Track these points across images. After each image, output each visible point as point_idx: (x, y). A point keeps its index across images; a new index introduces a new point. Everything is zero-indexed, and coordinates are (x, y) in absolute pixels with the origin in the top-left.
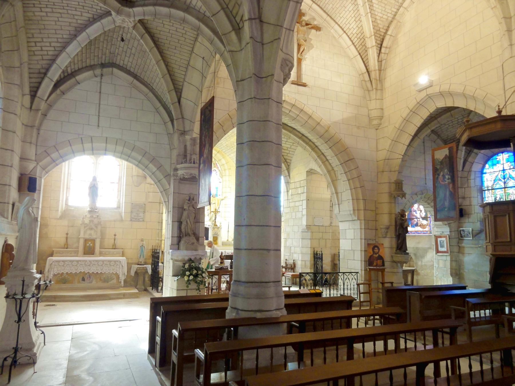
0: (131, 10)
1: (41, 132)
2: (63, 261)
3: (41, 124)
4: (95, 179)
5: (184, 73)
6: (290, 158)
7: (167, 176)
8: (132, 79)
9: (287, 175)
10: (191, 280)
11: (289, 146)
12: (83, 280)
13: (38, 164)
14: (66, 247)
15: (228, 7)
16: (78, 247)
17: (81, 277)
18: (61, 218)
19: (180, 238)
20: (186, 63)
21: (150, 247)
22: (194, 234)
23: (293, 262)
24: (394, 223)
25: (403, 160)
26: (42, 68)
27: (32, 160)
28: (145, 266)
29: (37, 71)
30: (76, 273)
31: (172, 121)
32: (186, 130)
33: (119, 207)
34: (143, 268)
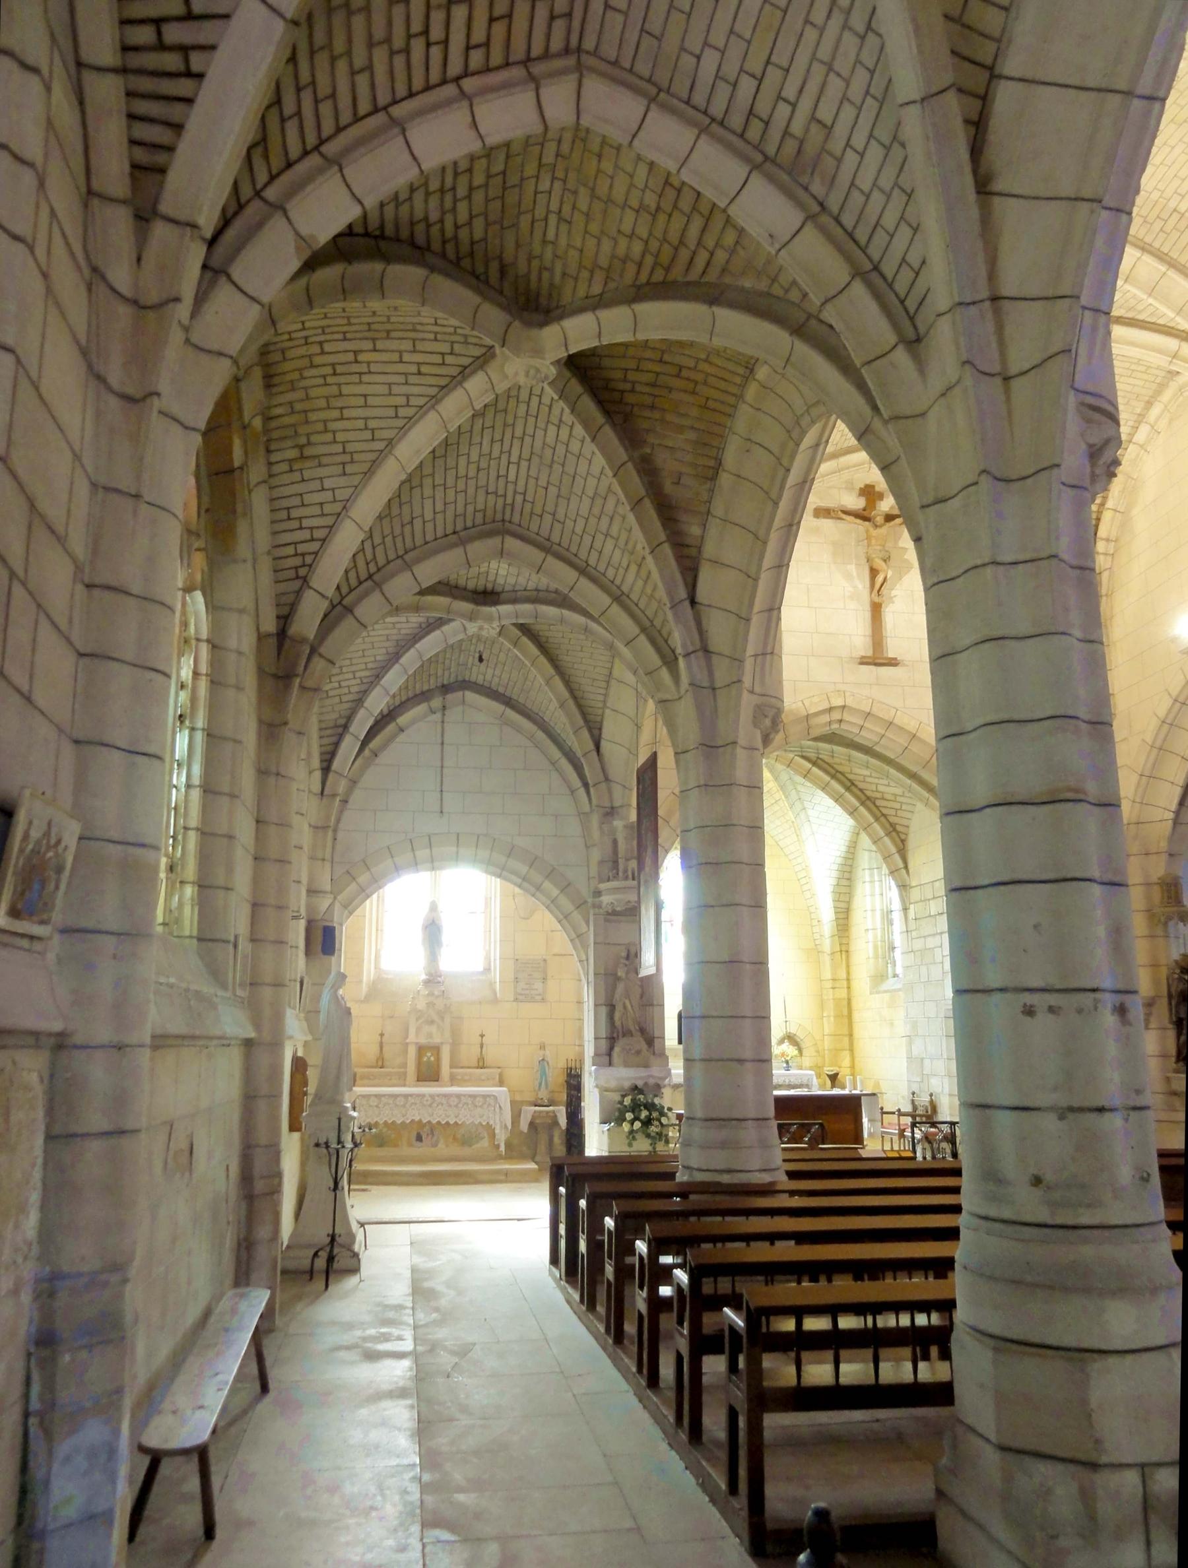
0: (493, 609)
1: (340, 835)
2: (376, 1096)
3: (338, 821)
4: (433, 908)
5: (603, 691)
6: (905, 822)
7: (580, 905)
8: (502, 707)
9: (901, 865)
10: (637, 1132)
12: (419, 1138)
13: (335, 898)
14: (380, 1063)
15: (653, 625)
16: (405, 1065)
17: (415, 1134)
18: (369, 998)
19: (612, 1040)
20: (606, 672)
21: (562, 1064)
22: (642, 1031)
23: (928, 1099)
24: (1165, 993)
25: (1176, 822)
26: (341, 717)
27: (325, 892)
28: (551, 1108)
29: (331, 724)
30: (403, 1123)
31: (586, 785)
32: (616, 804)
33: (487, 970)
34: (547, 1112)
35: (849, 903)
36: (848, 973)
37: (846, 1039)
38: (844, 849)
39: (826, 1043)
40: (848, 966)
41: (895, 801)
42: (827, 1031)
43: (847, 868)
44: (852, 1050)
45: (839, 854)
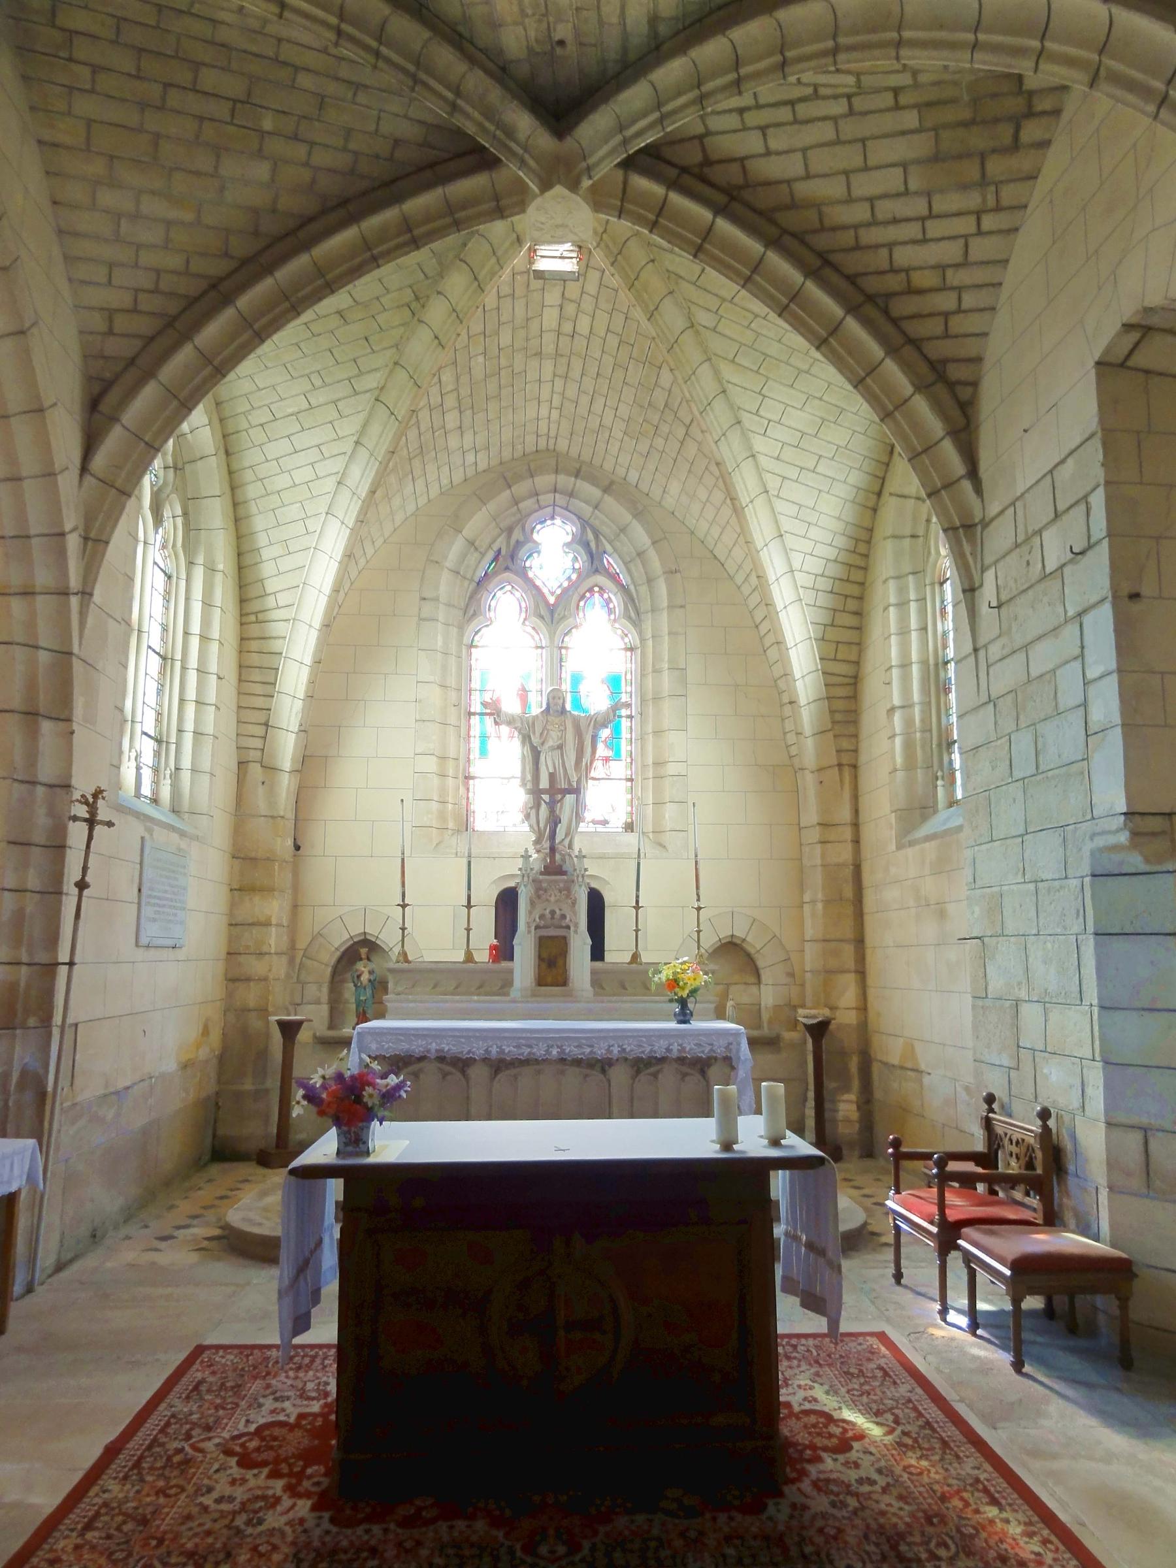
6: (969, 348)
11: (951, 252)
23: (1036, 1126)
35: (857, 663)
36: (856, 812)
37: (849, 950)
39: (808, 956)
40: (856, 797)
41: (944, 288)
42: (809, 933)
43: (854, 590)
44: (861, 973)
45: (832, 553)
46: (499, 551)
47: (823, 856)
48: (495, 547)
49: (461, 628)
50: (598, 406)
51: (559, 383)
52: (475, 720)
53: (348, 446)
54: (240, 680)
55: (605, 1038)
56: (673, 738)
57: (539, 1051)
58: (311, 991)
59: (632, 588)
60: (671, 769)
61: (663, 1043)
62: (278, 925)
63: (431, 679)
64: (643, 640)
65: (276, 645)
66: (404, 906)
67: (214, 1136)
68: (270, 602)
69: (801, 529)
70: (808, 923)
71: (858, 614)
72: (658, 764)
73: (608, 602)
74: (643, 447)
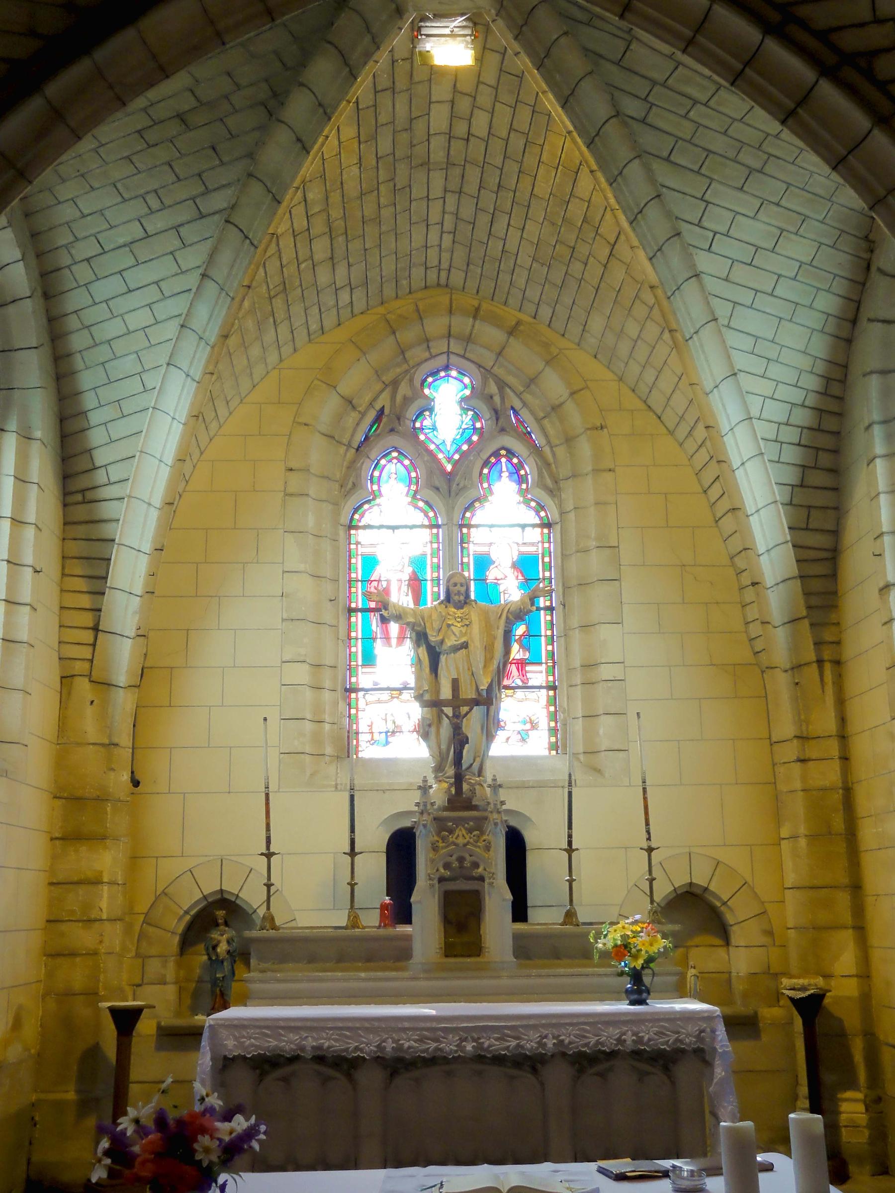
35: (836, 533)
36: (842, 720)
37: (843, 899)
38: (812, 383)
40: (841, 702)
42: (791, 879)
43: (825, 441)
44: (860, 929)
45: (797, 396)
46: (382, 410)
47: (804, 778)
48: (378, 406)
49: (337, 505)
50: (500, 226)
51: (451, 200)
52: (358, 619)
53: (193, 279)
54: (63, 575)
55: (535, 1027)
56: (606, 633)
57: (449, 1046)
58: (154, 967)
59: (547, 450)
60: (606, 672)
61: (615, 1032)
62: (111, 883)
63: (302, 567)
64: (562, 513)
65: (107, 530)
66: (269, 855)
67: (29, 1162)
68: (100, 477)
69: (758, 366)
70: (788, 864)
71: (834, 471)
72: (589, 666)
73: (517, 469)
74: (557, 276)
